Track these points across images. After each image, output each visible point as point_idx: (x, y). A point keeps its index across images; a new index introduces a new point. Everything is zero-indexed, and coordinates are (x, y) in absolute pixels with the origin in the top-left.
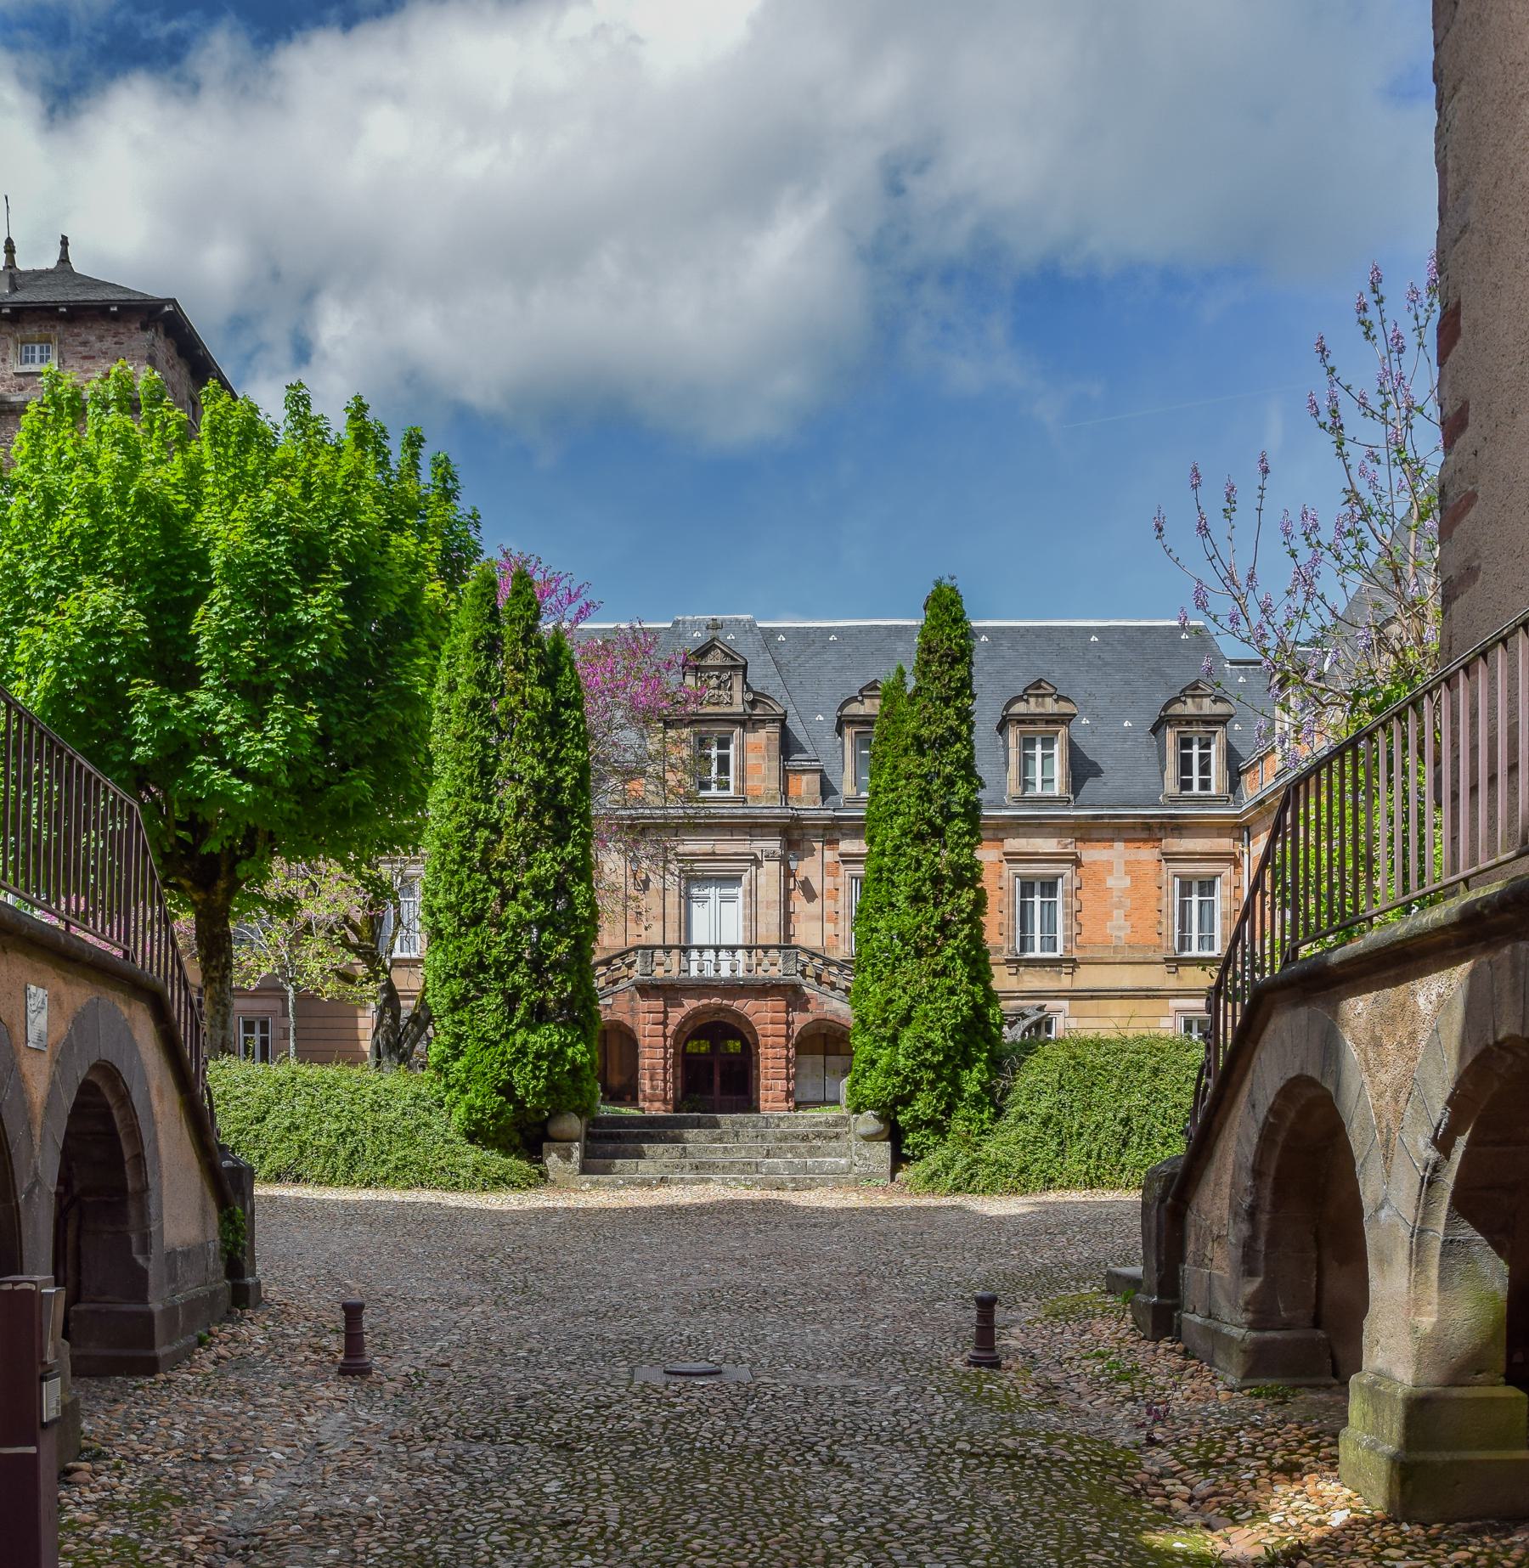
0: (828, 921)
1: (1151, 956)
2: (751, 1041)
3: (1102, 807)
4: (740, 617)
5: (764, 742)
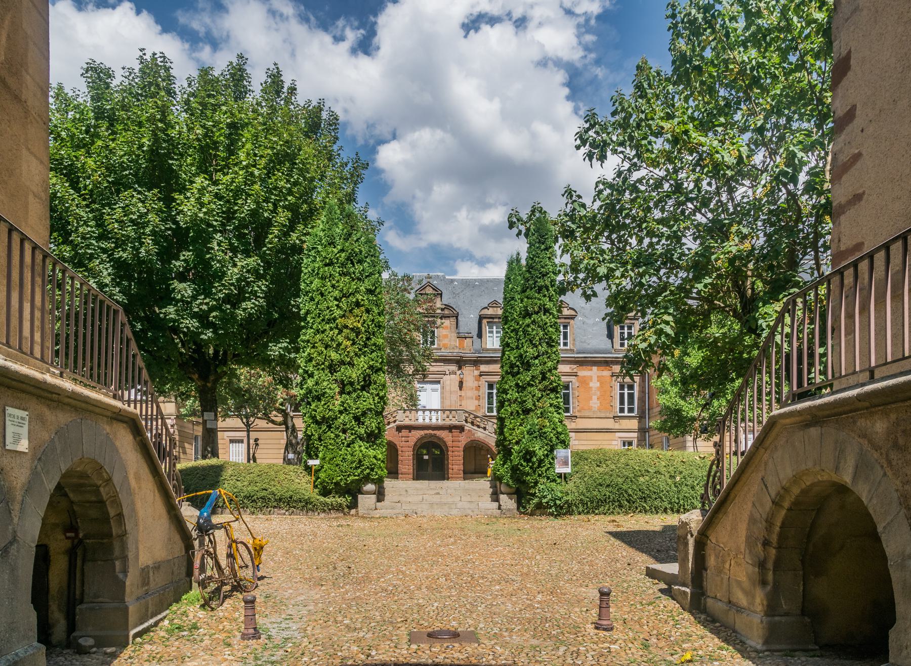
0: (476, 399)
1: (608, 415)
3: (588, 353)
4: (439, 274)
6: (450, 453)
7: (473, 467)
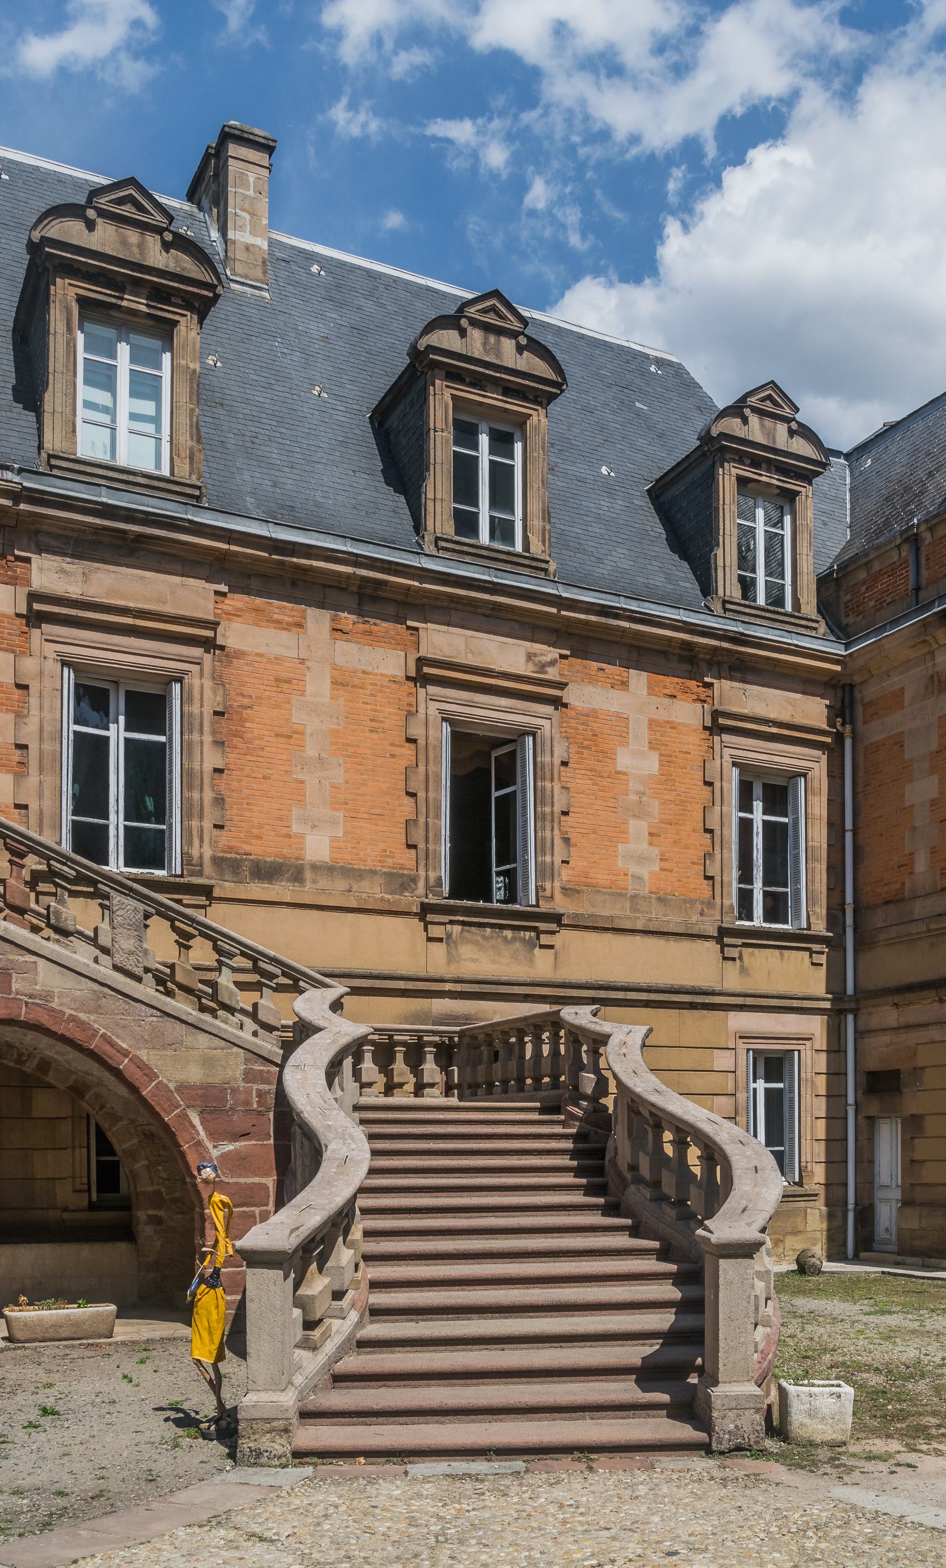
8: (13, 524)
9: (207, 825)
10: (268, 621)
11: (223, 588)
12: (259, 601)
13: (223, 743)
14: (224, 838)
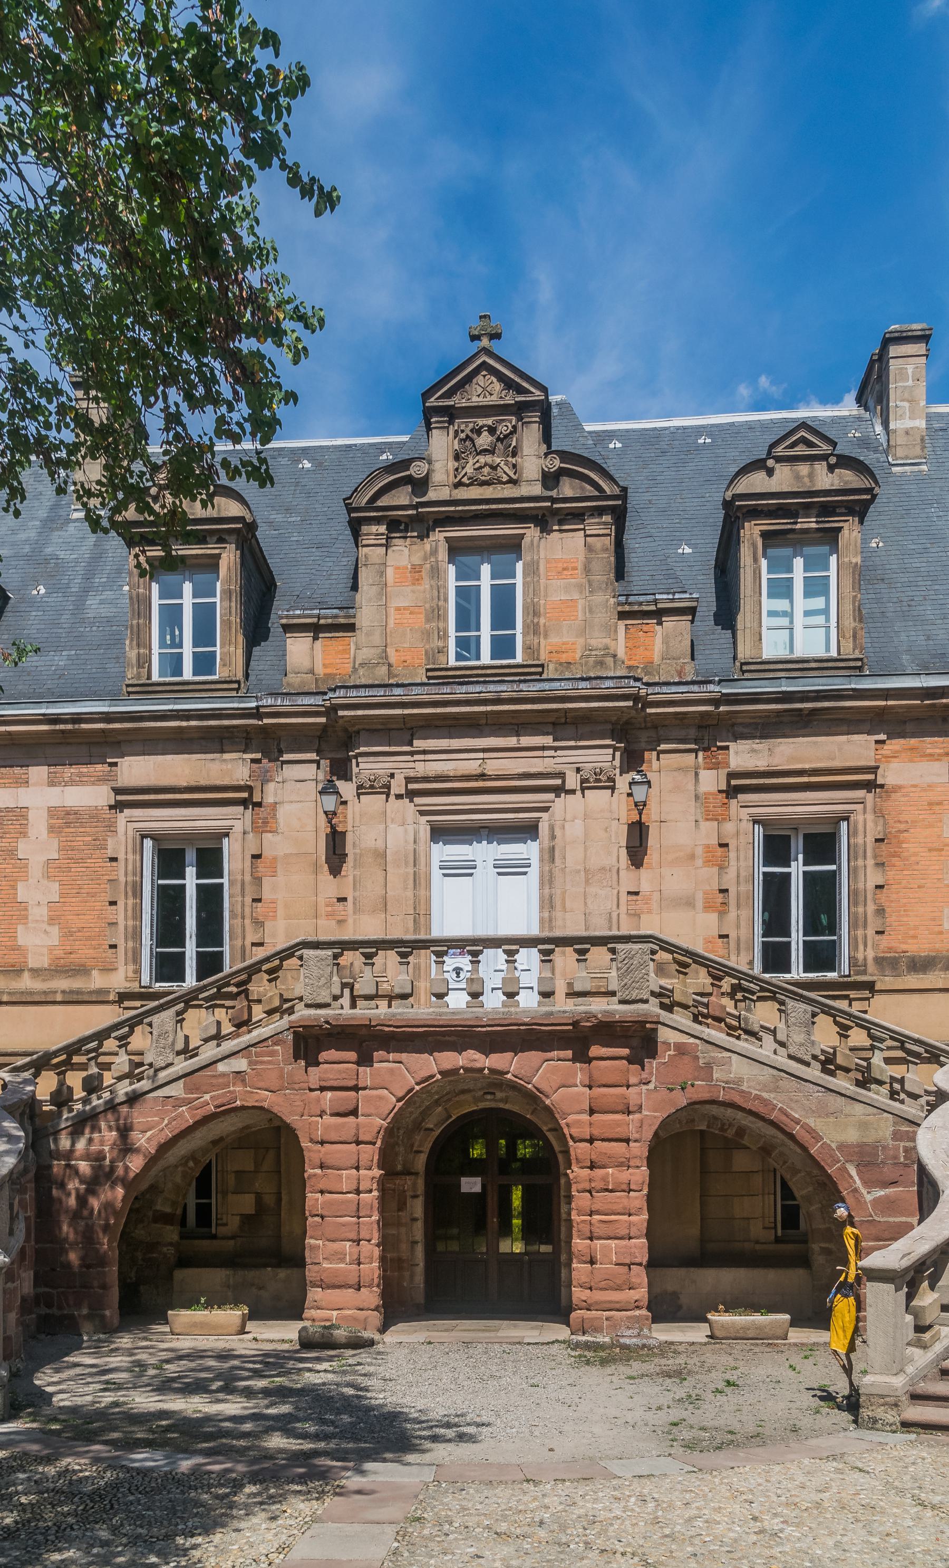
0: (708, 908)
2: (557, 1148)
5: (581, 557)
6: (577, 1173)
7: (694, 1231)
8: (715, 722)
9: (870, 932)
10: (921, 756)
11: (882, 737)
12: (913, 741)
13: (883, 864)
14: (884, 941)
